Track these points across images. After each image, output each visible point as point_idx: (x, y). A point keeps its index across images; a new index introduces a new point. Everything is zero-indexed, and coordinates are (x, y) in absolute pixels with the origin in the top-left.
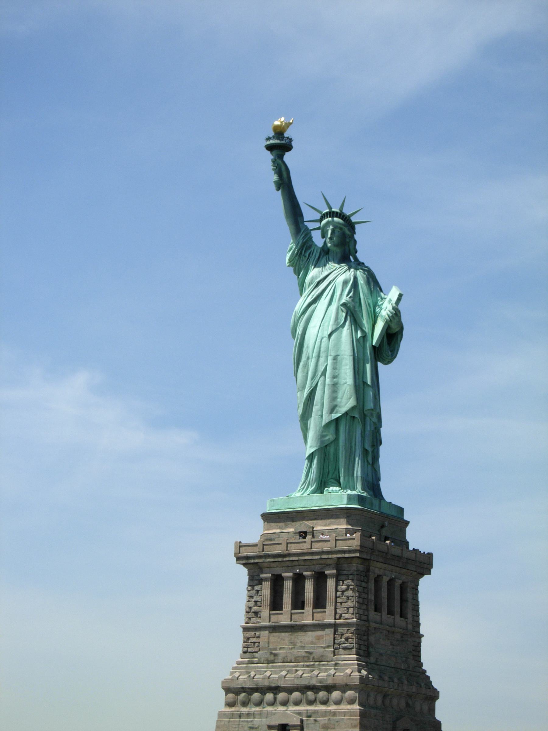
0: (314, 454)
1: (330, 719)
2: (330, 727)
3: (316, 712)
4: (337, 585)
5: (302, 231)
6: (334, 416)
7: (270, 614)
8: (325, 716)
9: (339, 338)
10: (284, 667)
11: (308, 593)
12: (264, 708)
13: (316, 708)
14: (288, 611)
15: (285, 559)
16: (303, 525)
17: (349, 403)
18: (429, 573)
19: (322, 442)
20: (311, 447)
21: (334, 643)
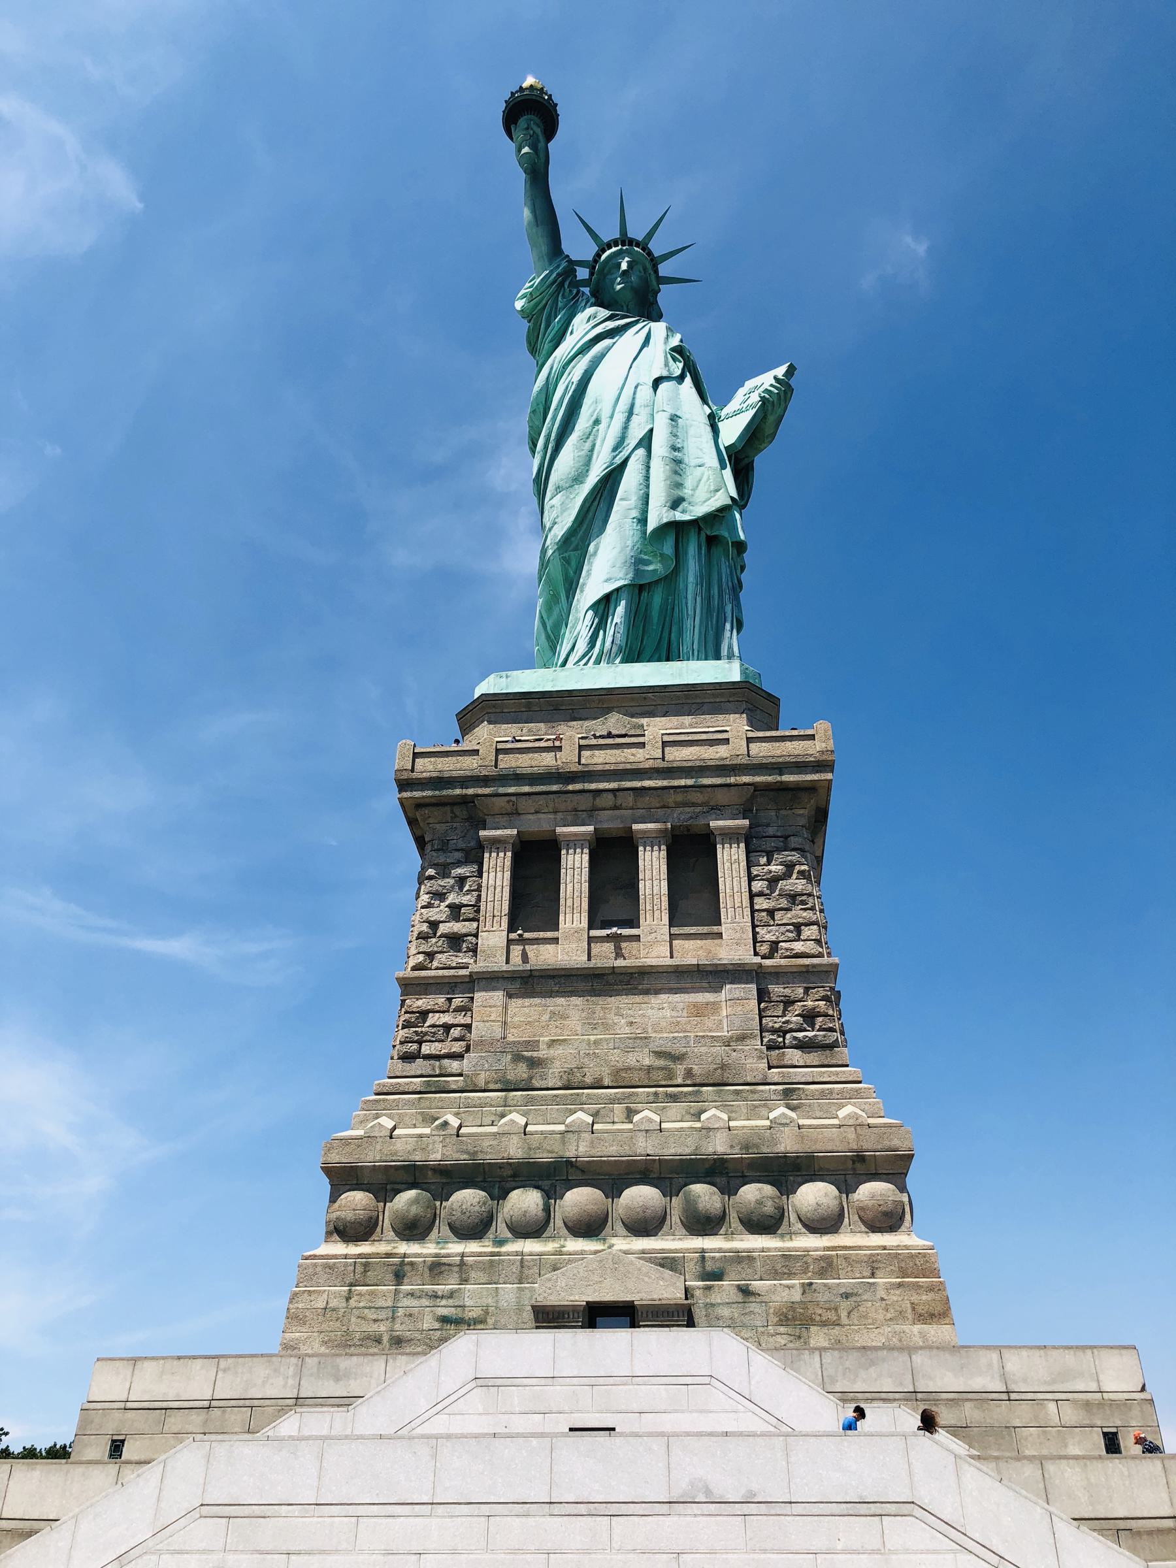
0: (614, 597)
1: (811, 1284)
2: (818, 1318)
6: (679, 516)
7: (510, 942)
8: (785, 1274)
12: (500, 1242)
15: (570, 787)
17: (713, 499)
19: (638, 573)
20: (607, 580)
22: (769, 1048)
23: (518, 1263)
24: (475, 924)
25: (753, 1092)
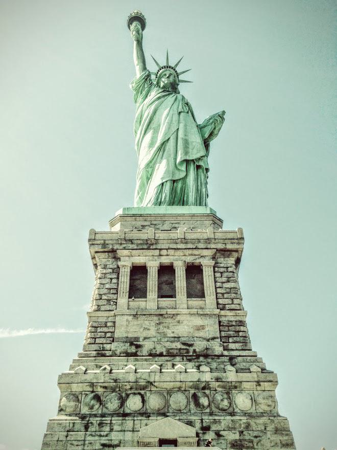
0: (165, 184)
6: (188, 158)
11: (179, 281)
12: (125, 415)
21: (221, 337)
22: (223, 342)
24: (116, 295)
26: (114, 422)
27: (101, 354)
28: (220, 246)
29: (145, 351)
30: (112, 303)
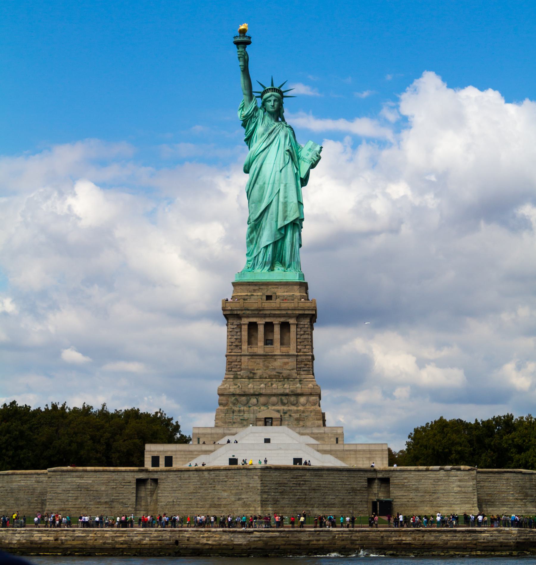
3: (289, 410)
4: (297, 331)
5: (254, 98)
6: (286, 222)
7: (248, 347)
9: (286, 172)
10: (262, 381)
12: (250, 407)
13: (289, 408)
14: (262, 346)
16: (269, 291)
18: (315, 322)
19: (275, 238)
20: (267, 241)
21: (297, 368)
23: (253, 411)
24: (241, 343)
25: (294, 381)
26: (245, 410)
27: (236, 378)
28: (301, 312)
29: (258, 376)
30: (239, 348)
